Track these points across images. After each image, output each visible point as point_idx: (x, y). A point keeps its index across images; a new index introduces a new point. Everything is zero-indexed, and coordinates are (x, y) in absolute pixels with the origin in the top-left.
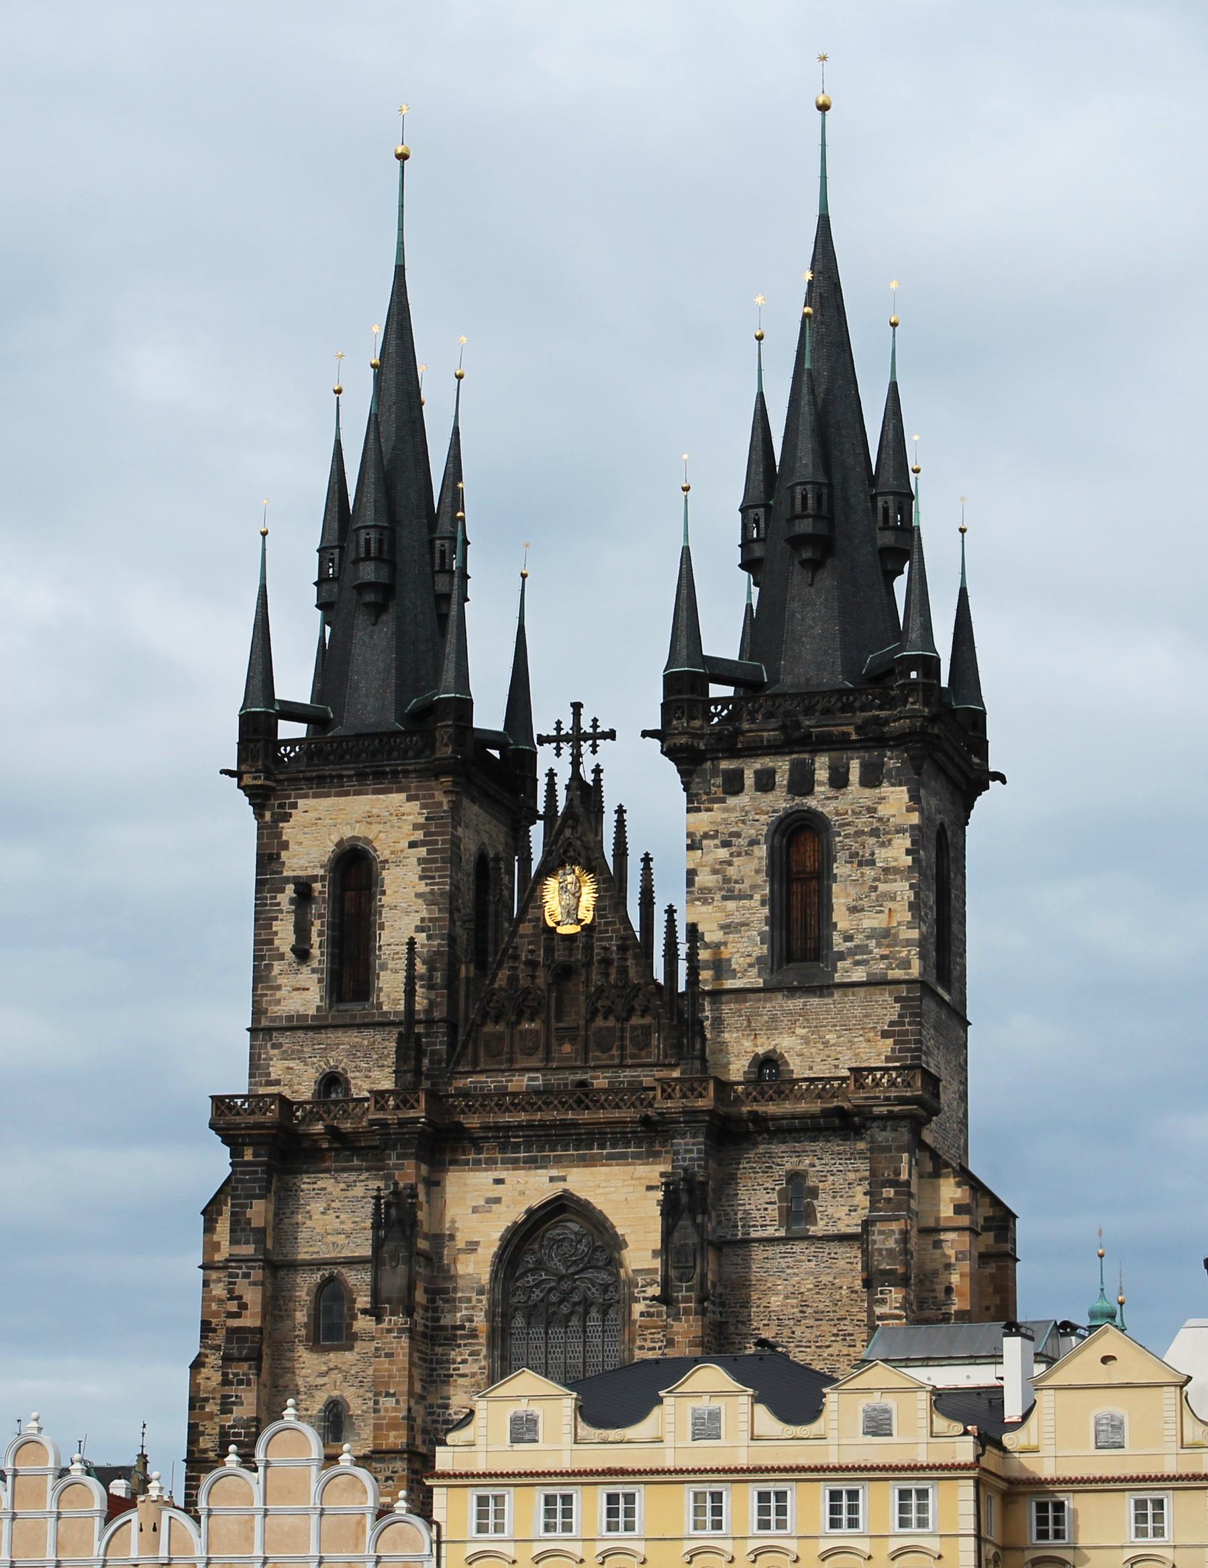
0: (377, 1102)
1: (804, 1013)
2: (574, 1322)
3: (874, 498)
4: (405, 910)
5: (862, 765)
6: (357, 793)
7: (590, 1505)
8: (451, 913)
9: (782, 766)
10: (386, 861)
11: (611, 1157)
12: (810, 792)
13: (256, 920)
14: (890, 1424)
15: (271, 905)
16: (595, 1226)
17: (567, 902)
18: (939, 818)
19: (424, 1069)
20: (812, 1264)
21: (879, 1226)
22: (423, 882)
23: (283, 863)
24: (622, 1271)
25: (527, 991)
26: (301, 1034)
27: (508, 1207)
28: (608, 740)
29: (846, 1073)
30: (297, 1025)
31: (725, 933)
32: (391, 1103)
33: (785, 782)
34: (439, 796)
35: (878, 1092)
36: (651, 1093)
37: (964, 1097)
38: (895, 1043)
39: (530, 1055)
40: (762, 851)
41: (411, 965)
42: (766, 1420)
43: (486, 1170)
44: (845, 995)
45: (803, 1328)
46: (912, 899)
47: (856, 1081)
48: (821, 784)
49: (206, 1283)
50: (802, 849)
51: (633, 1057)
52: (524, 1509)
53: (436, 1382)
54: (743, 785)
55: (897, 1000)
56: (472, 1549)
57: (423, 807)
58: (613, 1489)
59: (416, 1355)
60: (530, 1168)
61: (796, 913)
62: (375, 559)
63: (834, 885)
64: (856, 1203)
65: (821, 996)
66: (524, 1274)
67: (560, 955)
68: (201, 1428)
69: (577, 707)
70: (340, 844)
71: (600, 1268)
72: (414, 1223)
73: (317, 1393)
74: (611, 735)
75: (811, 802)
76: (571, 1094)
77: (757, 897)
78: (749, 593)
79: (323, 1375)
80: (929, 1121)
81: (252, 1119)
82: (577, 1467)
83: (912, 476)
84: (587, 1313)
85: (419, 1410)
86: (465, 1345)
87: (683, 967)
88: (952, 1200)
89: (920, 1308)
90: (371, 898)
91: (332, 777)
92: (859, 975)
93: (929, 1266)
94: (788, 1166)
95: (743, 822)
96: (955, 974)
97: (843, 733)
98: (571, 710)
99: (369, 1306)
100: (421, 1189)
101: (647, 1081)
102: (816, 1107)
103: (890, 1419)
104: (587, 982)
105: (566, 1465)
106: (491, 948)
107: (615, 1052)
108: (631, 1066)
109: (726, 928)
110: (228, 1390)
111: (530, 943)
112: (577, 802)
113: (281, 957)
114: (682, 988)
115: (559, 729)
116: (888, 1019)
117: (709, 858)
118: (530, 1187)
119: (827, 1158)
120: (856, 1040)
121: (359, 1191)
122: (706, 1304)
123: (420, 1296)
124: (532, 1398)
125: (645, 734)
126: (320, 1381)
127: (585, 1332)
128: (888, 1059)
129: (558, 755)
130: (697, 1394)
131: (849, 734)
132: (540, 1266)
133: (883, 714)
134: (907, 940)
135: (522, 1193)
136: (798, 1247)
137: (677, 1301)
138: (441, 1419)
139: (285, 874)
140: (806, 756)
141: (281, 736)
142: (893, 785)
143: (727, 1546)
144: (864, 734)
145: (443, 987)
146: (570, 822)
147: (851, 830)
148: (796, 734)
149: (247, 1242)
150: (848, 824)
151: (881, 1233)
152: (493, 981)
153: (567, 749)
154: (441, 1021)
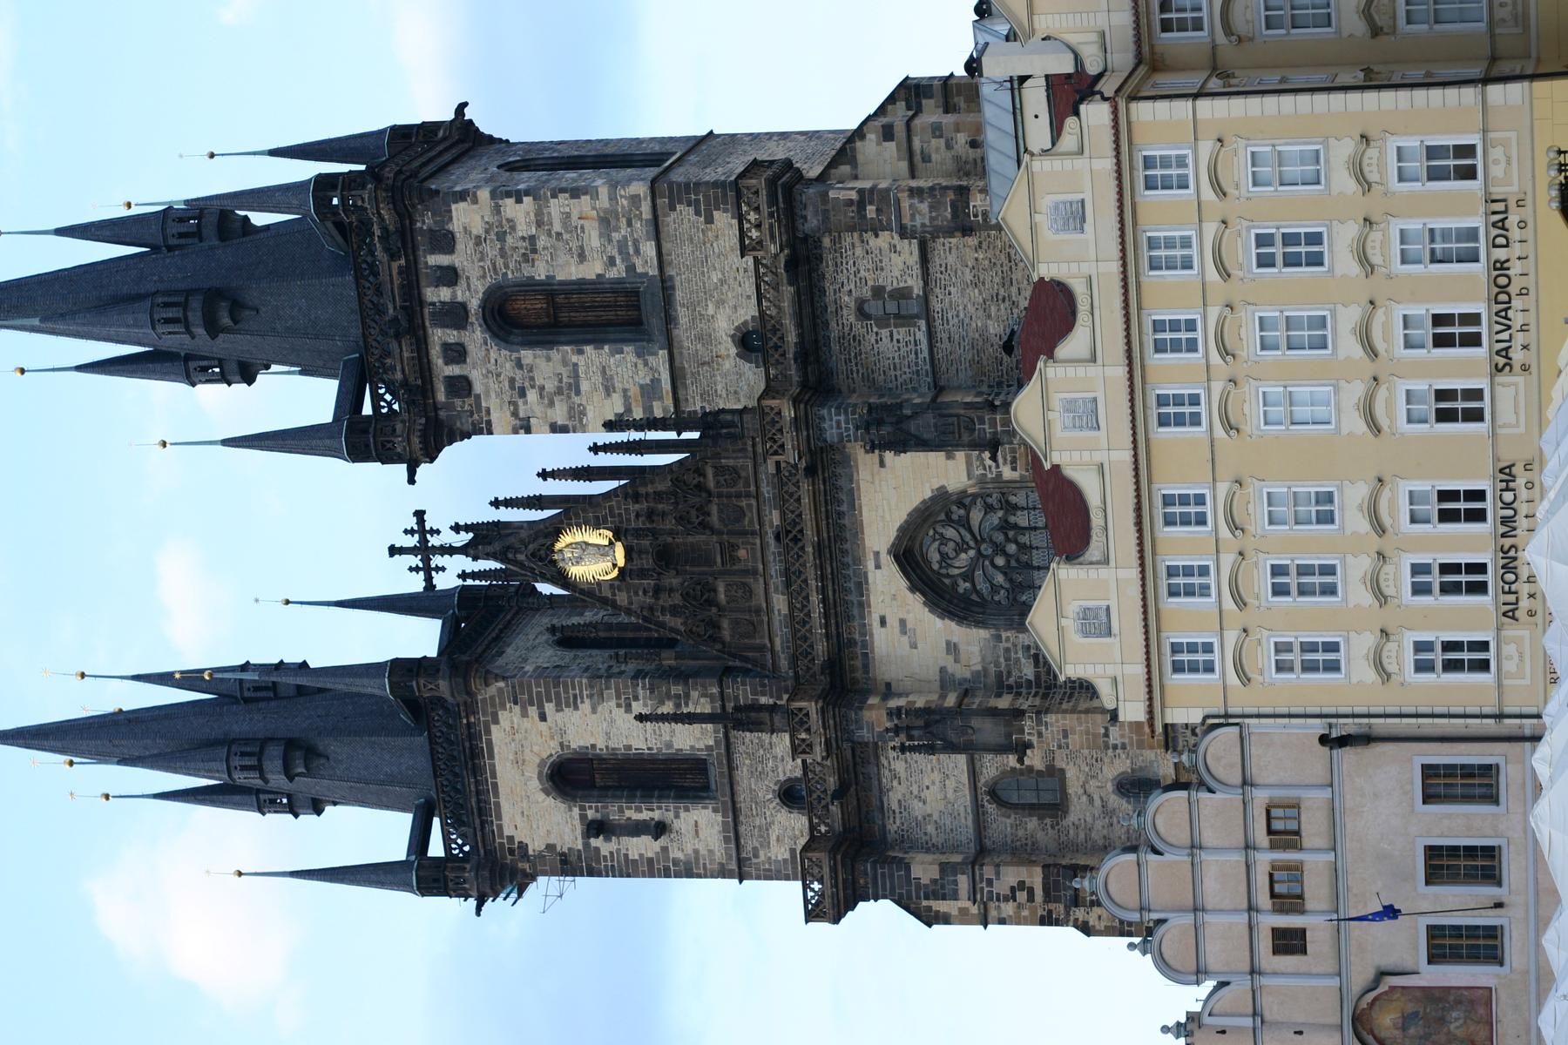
1: (692, 306)
2: (1024, 539)
3: (170, 249)
4: (608, 724)
5: (432, 253)
6: (494, 775)
7: (1179, 545)
8: (609, 677)
9: (439, 336)
10: (561, 744)
11: (852, 505)
12: (463, 306)
13: (629, 876)
16: (925, 521)
17: (592, 557)
19: (771, 701)
20: (953, 290)
21: (906, 221)
24: (970, 491)
25: (686, 596)
26: (742, 829)
29: (749, 260)
30: (734, 833)
32: (803, 736)
34: (492, 690)
35: (766, 226)
37: (784, 136)
39: (751, 592)
40: (527, 355)
41: (664, 718)
42: (1074, 345)
43: (872, 635)
44: (670, 263)
47: (754, 249)
48: (454, 295)
49: (1002, 921)
51: (747, 484)
52: (1186, 620)
55: (673, 208)
57: (503, 707)
58: (1159, 520)
59: (1064, 706)
61: (591, 316)
62: (260, 760)
64: (885, 246)
65: (673, 288)
66: (978, 593)
67: (647, 562)
69: (394, 551)
70: (548, 794)
72: (926, 711)
74: (420, 515)
75: (474, 304)
76: (787, 550)
77: (575, 359)
79: (1091, 800)
80: (798, 170)
82: (1135, 562)
84: (1015, 527)
87: (653, 435)
88: (878, 144)
90: (601, 759)
91: (479, 801)
92: (649, 249)
93: (950, 165)
94: (852, 319)
95: (498, 375)
96: (657, 148)
97: (400, 273)
100: (894, 703)
101: (771, 469)
102: (788, 291)
104: (671, 533)
105: (1134, 573)
106: (645, 634)
107: (744, 503)
108: (757, 487)
109: (609, 390)
111: (636, 594)
112: (489, 549)
113: (665, 849)
115: (416, 569)
116: (694, 218)
118: (887, 590)
119: (842, 278)
121: (899, 766)
122: (997, 403)
123: (1004, 703)
124: (1060, 614)
125: (411, 481)
127: (1035, 529)
129: (443, 569)
130: (1047, 426)
133: (377, 232)
136: (936, 305)
137: (995, 433)
139: (580, 847)
140: (426, 311)
141: (442, 854)
142: (451, 218)
145: (686, 684)
146: (510, 556)
147: (500, 262)
148: (404, 323)
149: (955, 883)
151: (913, 217)
152: (677, 632)
153: (437, 560)
154: (721, 686)
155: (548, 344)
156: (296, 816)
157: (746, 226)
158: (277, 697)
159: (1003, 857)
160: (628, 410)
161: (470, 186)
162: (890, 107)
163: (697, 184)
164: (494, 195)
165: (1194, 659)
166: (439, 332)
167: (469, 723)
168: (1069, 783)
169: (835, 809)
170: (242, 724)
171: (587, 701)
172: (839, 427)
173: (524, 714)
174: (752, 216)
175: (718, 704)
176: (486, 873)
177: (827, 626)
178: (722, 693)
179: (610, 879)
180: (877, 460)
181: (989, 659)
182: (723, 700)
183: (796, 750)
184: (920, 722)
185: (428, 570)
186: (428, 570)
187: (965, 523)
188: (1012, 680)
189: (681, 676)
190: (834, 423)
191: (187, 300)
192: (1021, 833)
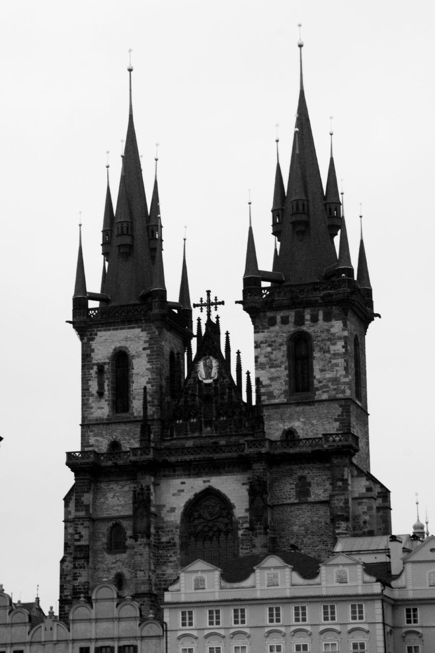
0: (133, 453)
2: (215, 538)
5: (323, 313)
6: (121, 329)
7: (227, 615)
8: (161, 376)
9: (292, 315)
10: (133, 356)
12: (303, 324)
13: (82, 381)
14: (346, 578)
15: (88, 374)
18: (355, 333)
19: (152, 439)
21: (336, 497)
22: (149, 364)
23: (92, 358)
24: (233, 518)
27: (187, 493)
28: (222, 305)
29: (320, 436)
30: (99, 423)
32: (139, 452)
33: (293, 320)
34: (154, 329)
35: (334, 444)
36: (243, 446)
37: (367, 444)
38: (340, 423)
40: (284, 348)
42: (297, 579)
43: (178, 478)
45: (307, 539)
46: (345, 365)
47: (325, 439)
48: (307, 320)
49: (66, 528)
52: (201, 618)
53: (160, 565)
54: (276, 322)
56: (180, 633)
57: (148, 333)
59: (151, 554)
60: (195, 477)
62: (125, 234)
64: (326, 487)
65: (310, 405)
66: (194, 520)
68: (65, 587)
69: (209, 292)
70: (114, 350)
71: (225, 516)
72: (149, 501)
73: (112, 571)
74: (223, 303)
75: (304, 328)
76: (212, 447)
77: (283, 366)
78: (276, 244)
80: (355, 455)
81: (83, 461)
83: (340, 196)
84: (220, 535)
85: (153, 577)
86: (171, 549)
88: (365, 486)
89: (354, 530)
91: (111, 323)
92: (325, 396)
93: (357, 513)
94: (299, 474)
95: (277, 337)
96: (363, 395)
97: (316, 300)
98: (206, 293)
99: (132, 535)
100: (152, 487)
101: (242, 441)
102: (310, 450)
103: (346, 576)
105: (217, 597)
108: (235, 435)
110: (75, 571)
113: (93, 395)
114: (254, 403)
115: (201, 301)
116: (337, 414)
117: (264, 351)
118: (197, 485)
119: (314, 470)
120: (325, 422)
121: (126, 488)
122: (268, 530)
123: (153, 530)
124: (203, 571)
125: (237, 302)
126: (113, 566)
127: (219, 543)
128: (337, 430)
129: (202, 311)
132: (200, 517)
133: (332, 292)
135: (192, 488)
136: (304, 506)
137: (256, 529)
138: (162, 579)
139: (93, 362)
140: (301, 309)
142: (336, 320)
143: (283, 629)
149: (82, 511)
153: (205, 309)
154: (158, 419)
155: (289, 356)
156: (102, 245)
157: (334, 436)
158: (150, 239)
159: (91, 529)
160: (264, 386)
161: (349, 326)
162: (379, 485)
163: (350, 415)
164: (345, 337)
165: (187, 619)
167: (142, 320)
168: (120, 555)
169: (110, 463)
170: (139, 226)
171: (151, 367)
172: (258, 469)
173: (145, 342)
174: (337, 439)
175: (150, 418)
176: (83, 325)
177: (181, 462)
178: (155, 420)
179: (81, 373)
180: (245, 482)
181: (168, 524)
182: (152, 420)
183: (134, 450)
184: (145, 498)
185: (201, 305)
186: (201, 305)
187: (221, 516)
188: (160, 533)
189: (160, 405)
190: (259, 468)
192: (101, 535)
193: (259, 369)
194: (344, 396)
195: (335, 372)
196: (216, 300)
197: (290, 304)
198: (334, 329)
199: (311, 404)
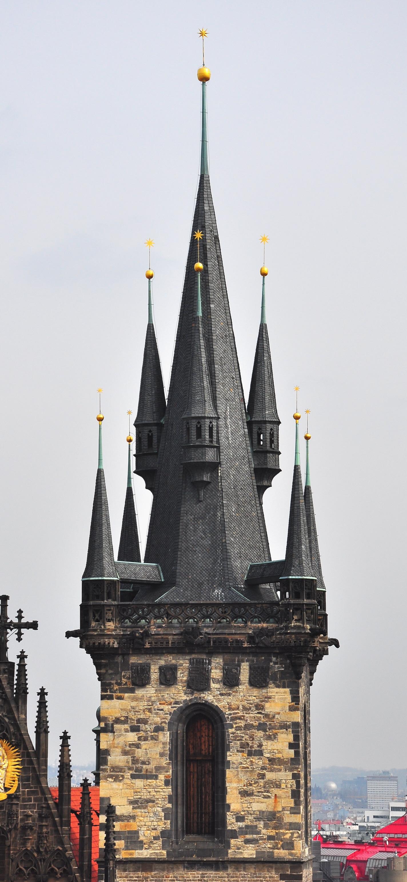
5: (252, 668)
12: (206, 688)
28: (31, 630)
31: (134, 808)
40: (165, 737)
44: (237, 869)
46: (294, 787)
50: (198, 735)
54: (149, 678)
63: (228, 772)
65: (217, 869)
74: (34, 625)
75: (208, 697)
77: (162, 777)
78: (129, 478)
92: (249, 852)
95: (150, 710)
97: (237, 641)
109: (135, 803)
125: (69, 634)
131: (242, 642)
134: (291, 824)
142: (278, 686)
144: (254, 643)
150: (240, 718)
155: (173, 756)
166: (186, 664)
191: (214, 447)
193: (110, 780)
194: (291, 854)
195: (271, 801)
196: (20, 617)
197: (182, 645)
198: (273, 704)
199: (220, 866)
